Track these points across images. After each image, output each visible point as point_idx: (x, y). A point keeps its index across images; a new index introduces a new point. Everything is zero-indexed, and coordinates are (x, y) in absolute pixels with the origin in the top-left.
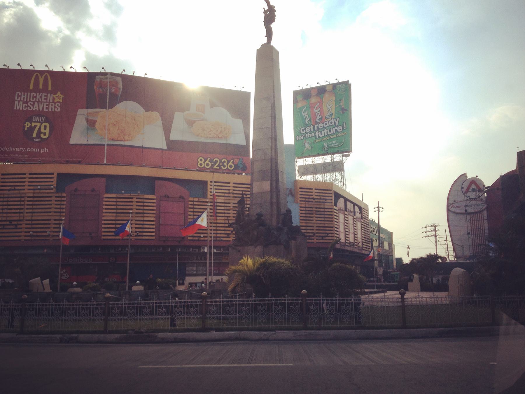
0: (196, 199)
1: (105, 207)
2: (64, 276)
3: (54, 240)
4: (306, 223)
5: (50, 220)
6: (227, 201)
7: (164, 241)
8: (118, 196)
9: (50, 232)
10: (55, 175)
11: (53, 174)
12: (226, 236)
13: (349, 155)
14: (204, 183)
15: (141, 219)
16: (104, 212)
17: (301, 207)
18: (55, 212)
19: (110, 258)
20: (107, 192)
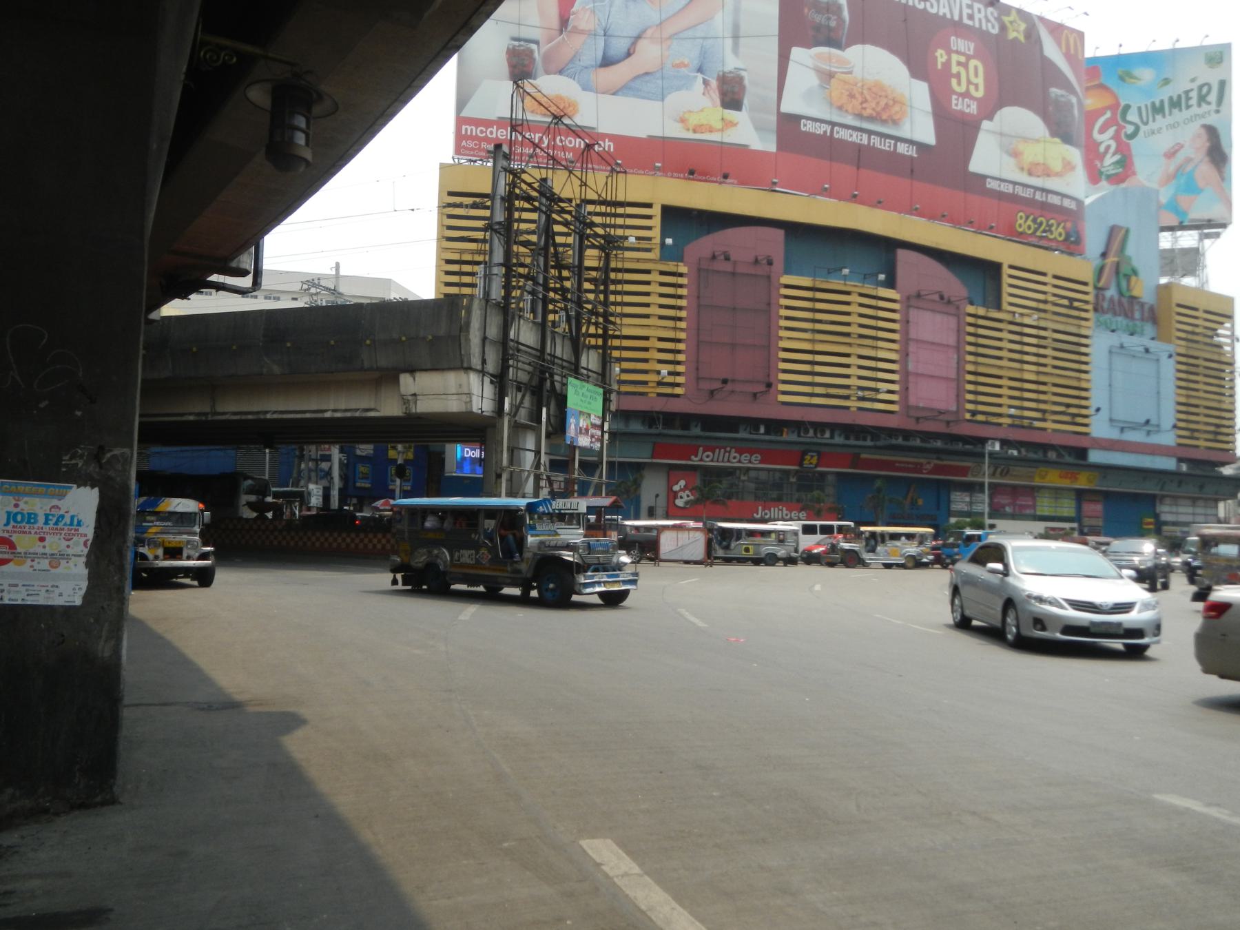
1: (783, 312)
2: (681, 497)
3: (659, 395)
4: (1188, 396)
5: (646, 338)
6: (1042, 324)
7: (918, 419)
9: (659, 372)
10: (656, 211)
11: (649, 206)
12: (1038, 415)
13: (1217, 235)
14: (988, 271)
15: (871, 353)
18: (661, 317)
20: (788, 271)
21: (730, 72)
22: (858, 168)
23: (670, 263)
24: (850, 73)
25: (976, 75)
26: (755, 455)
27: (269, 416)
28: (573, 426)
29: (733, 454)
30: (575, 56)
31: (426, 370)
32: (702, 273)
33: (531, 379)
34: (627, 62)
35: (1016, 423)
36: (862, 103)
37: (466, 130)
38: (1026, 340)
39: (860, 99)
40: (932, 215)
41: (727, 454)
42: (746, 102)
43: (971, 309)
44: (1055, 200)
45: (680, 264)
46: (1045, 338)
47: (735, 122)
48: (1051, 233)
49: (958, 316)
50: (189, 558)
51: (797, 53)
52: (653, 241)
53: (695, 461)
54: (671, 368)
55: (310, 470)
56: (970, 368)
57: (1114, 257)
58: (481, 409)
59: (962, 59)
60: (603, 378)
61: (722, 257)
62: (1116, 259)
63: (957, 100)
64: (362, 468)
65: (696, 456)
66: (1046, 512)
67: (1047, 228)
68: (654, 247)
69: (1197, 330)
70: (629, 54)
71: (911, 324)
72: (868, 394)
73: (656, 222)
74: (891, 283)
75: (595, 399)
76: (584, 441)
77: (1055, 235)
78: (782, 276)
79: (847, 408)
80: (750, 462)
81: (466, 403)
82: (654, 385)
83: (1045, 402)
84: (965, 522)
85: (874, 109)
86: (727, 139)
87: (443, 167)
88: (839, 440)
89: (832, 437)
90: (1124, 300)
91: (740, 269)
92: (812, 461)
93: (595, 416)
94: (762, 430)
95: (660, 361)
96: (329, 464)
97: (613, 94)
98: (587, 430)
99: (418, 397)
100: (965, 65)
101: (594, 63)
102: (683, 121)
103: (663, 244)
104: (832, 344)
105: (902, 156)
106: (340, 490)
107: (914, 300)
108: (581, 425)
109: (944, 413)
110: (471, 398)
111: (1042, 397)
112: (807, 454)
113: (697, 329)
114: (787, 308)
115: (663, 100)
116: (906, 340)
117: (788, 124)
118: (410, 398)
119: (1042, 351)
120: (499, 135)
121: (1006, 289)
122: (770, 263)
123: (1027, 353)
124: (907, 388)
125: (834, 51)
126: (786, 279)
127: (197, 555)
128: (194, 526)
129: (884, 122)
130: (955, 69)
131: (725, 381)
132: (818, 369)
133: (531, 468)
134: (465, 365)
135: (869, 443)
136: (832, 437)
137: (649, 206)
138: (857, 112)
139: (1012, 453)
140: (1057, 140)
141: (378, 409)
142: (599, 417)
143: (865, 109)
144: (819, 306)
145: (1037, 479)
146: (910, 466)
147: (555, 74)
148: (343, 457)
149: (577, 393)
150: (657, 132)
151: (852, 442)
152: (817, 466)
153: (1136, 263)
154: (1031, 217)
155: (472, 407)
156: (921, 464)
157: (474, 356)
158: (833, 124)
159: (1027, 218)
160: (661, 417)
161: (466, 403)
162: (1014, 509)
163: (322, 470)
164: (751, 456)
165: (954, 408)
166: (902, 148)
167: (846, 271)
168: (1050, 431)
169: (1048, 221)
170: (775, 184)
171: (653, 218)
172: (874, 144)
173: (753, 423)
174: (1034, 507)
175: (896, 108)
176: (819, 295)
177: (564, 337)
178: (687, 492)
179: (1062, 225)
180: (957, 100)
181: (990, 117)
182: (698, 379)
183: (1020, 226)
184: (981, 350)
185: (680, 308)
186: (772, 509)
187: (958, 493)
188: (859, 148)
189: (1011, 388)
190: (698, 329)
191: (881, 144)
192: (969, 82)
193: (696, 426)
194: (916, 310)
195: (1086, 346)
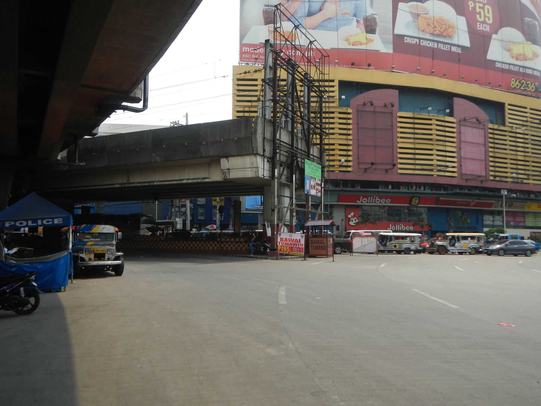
0: (496, 127)
1: (399, 130)
2: (352, 221)
3: (340, 171)
6: (526, 132)
7: (467, 180)
8: (415, 115)
9: (340, 161)
10: (336, 83)
16: (399, 137)
18: (340, 134)
19: (413, 200)
20: (400, 110)
21: (370, 16)
22: (433, 59)
23: (343, 108)
24: (428, 14)
25: (488, 13)
26: (388, 200)
27: (155, 183)
28: (308, 184)
29: (377, 199)
30: (295, 12)
31: (234, 156)
32: (359, 112)
33: (287, 160)
34: (320, 13)
35: (515, 181)
36: (433, 28)
37: (245, 49)
38: (518, 140)
39: (433, 27)
40: (469, 81)
41: (374, 199)
42: (377, 30)
43: (491, 126)
44: (529, 72)
45: (348, 108)
46: (527, 139)
47: (372, 40)
48: (528, 88)
49: (484, 129)
50: (109, 259)
51: (401, 5)
52: (335, 98)
53: (359, 203)
54: (345, 158)
55: (176, 212)
56: (491, 154)
58: (263, 175)
59: (481, 5)
60: (320, 160)
61: (369, 104)
63: (480, 25)
64: (200, 210)
65: (359, 201)
66: (530, 225)
67: (526, 86)
68: (335, 100)
70: (320, 10)
71: (461, 133)
72: (443, 168)
73: (336, 89)
74: (451, 114)
75: (318, 171)
76: (313, 192)
77: (530, 88)
78: (398, 112)
79: (432, 175)
80: (385, 203)
81: (255, 172)
82: (338, 167)
83: (528, 170)
84: (494, 230)
85: (439, 31)
86: (368, 48)
87: (234, 67)
88: (428, 191)
89: (425, 189)
91: (378, 110)
92: (416, 202)
93: (318, 179)
94: (390, 187)
95: (340, 155)
96: (185, 209)
97: (313, 29)
98: (314, 186)
99: (230, 170)
100: (483, 8)
101: (304, 15)
102: (347, 40)
103: (340, 99)
104: (423, 144)
105: (454, 53)
106: (190, 221)
107: (463, 122)
108: (312, 184)
109: (481, 177)
110: (258, 169)
111: (527, 168)
112: (413, 198)
113: (358, 140)
114: (401, 127)
115: (337, 31)
116: (460, 142)
117: (398, 39)
118: (226, 171)
119: (526, 145)
120: (260, 51)
121: (507, 116)
122: (393, 106)
123: (518, 147)
124: (461, 165)
125: (419, 4)
126: (400, 114)
127: (113, 257)
128: (113, 241)
129: (445, 37)
130: (478, 10)
131: (372, 164)
132: (417, 157)
133: (289, 206)
134: (255, 152)
135: (442, 192)
136: (425, 189)
137: (333, 81)
138: (431, 33)
139: (513, 196)
140: (529, 43)
141: (210, 178)
142: (319, 180)
143: (435, 31)
144: (417, 126)
145: (526, 208)
146: (464, 203)
147: (286, 21)
148: (192, 205)
149: (309, 167)
150: (335, 46)
151: (434, 192)
152: (418, 204)
154: (518, 80)
155: (259, 174)
156: (469, 202)
157: (259, 147)
158: (420, 39)
159: (516, 81)
160: (342, 182)
161: (255, 172)
162: (515, 223)
163: (182, 212)
164: (386, 200)
165: (484, 174)
166: (454, 49)
167: (430, 109)
168: (531, 184)
169: (526, 82)
170: (393, 68)
171: (335, 86)
172: (440, 47)
173: (386, 184)
174: (524, 222)
175: (451, 30)
176: (416, 121)
177: (302, 139)
178: (355, 218)
179: (534, 83)
180: (480, 25)
181: (496, 33)
182: (359, 163)
183: (513, 85)
184: (497, 146)
185: (349, 129)
186: (396, 225)
187: (487, 216)
188: (433, 49)
189: (511, 164)
190: (358, 139)
191: (443, 48)
192: (485, 16)
193: (358, 186)
194: (464, 127)
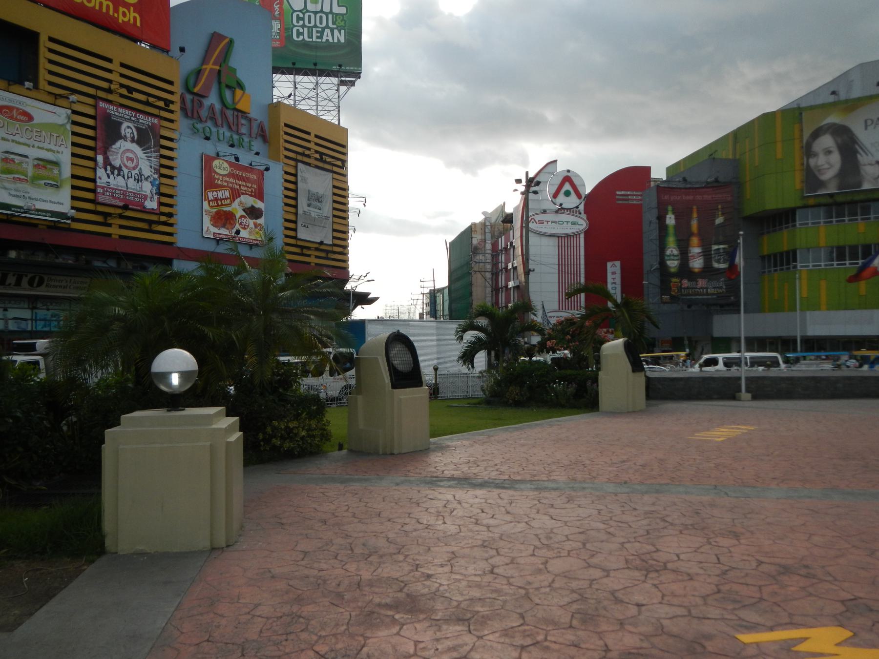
12: (99, 219)
13: (353, 84)
17: (286, 173)
57: (214, 64)
62: (218, 68)
69: (307, 152)
90: (229, 113)
153: (241, 75)
195: (171, 149)
